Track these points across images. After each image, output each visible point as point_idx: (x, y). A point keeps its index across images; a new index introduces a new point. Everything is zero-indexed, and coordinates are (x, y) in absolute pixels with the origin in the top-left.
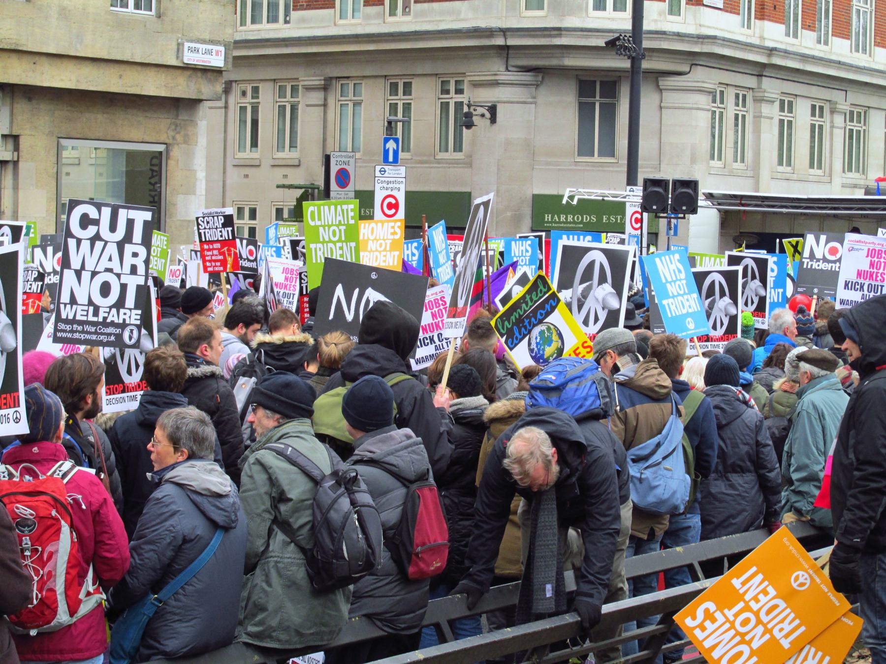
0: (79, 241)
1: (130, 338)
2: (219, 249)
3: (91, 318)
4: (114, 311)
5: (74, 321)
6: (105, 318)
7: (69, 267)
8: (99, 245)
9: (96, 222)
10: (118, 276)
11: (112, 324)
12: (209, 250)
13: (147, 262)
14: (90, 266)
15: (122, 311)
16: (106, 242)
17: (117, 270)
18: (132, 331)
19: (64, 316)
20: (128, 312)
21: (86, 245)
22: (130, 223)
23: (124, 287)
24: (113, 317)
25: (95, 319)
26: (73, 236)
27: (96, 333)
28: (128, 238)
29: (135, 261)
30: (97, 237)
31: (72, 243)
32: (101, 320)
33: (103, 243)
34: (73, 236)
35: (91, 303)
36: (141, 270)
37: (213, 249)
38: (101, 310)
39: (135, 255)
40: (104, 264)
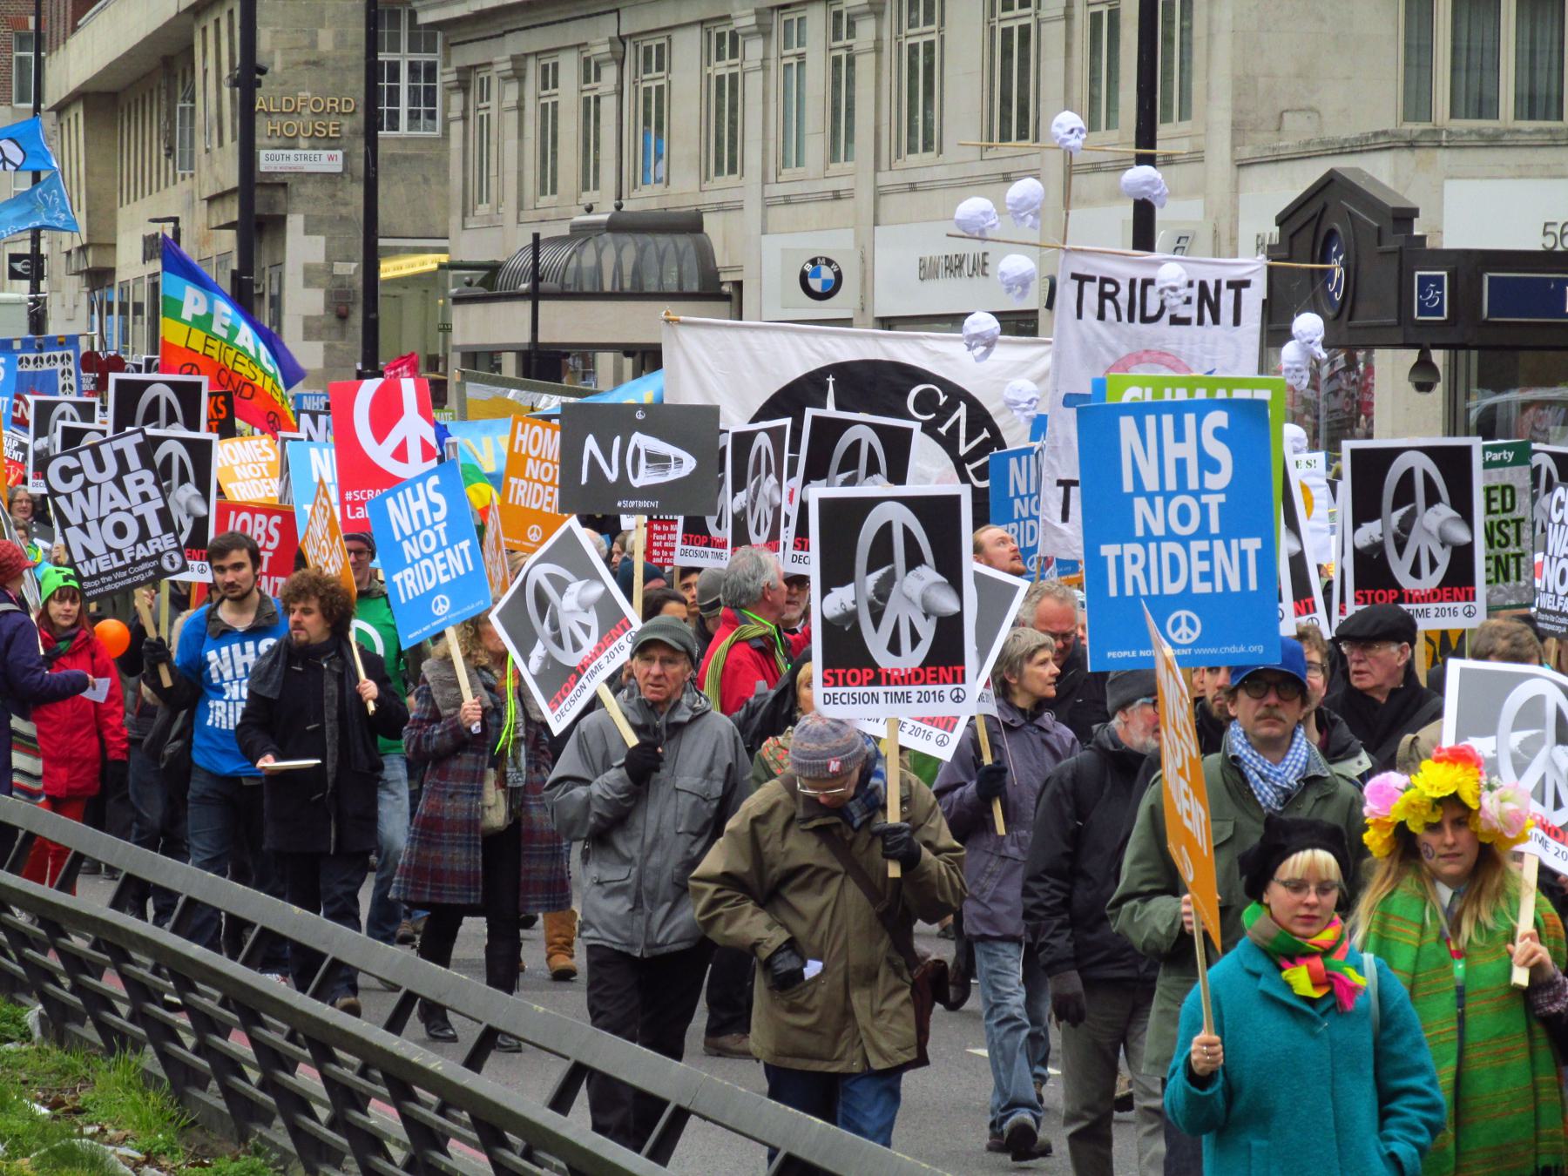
3: (117, 564)
4: (140, 546)
6: (133, 558)
11: (144, 559)
14: (92, 514)
24: (142, 552)
25: (122, 563)
26: (60, 494)
27: (129, 576)
31: (61, 501)
34: (60, 494)
35: (110, 550)
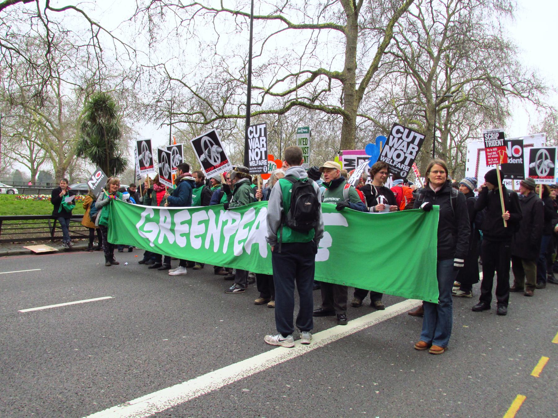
0: (394, 137)
1: (403, 175)
2: (496, 151)
3: (390, 163)
4: (399, 164)
6: (395, 165)
7: (388, 144)
8: (401, 141)
9: (402, 133)
10: (405, 153)
11: (398, 168)
12: (490, 152)
13: (417, 152)
14: (395, 146)
15: (402, 165)
16: (403, 141)
17: (405, 151)
18: (404, 173)
19: (381, 160)
20: (405, 166)
21: (396, 139)
22: (415, 138)
23: (405, 158)
24: (399, 165)
25: (392, 164)
26: (392, 135)
28: (413, 142)
29: (412, 150)
30: (401, 138)
31: (391, 137)
32: (394, 165)
33: (402, 141)
35: (392, 158)
36: (414, 154)
37: (493, 151)
38: (395, 162)
39: (413, 148)
40: (401, 147)
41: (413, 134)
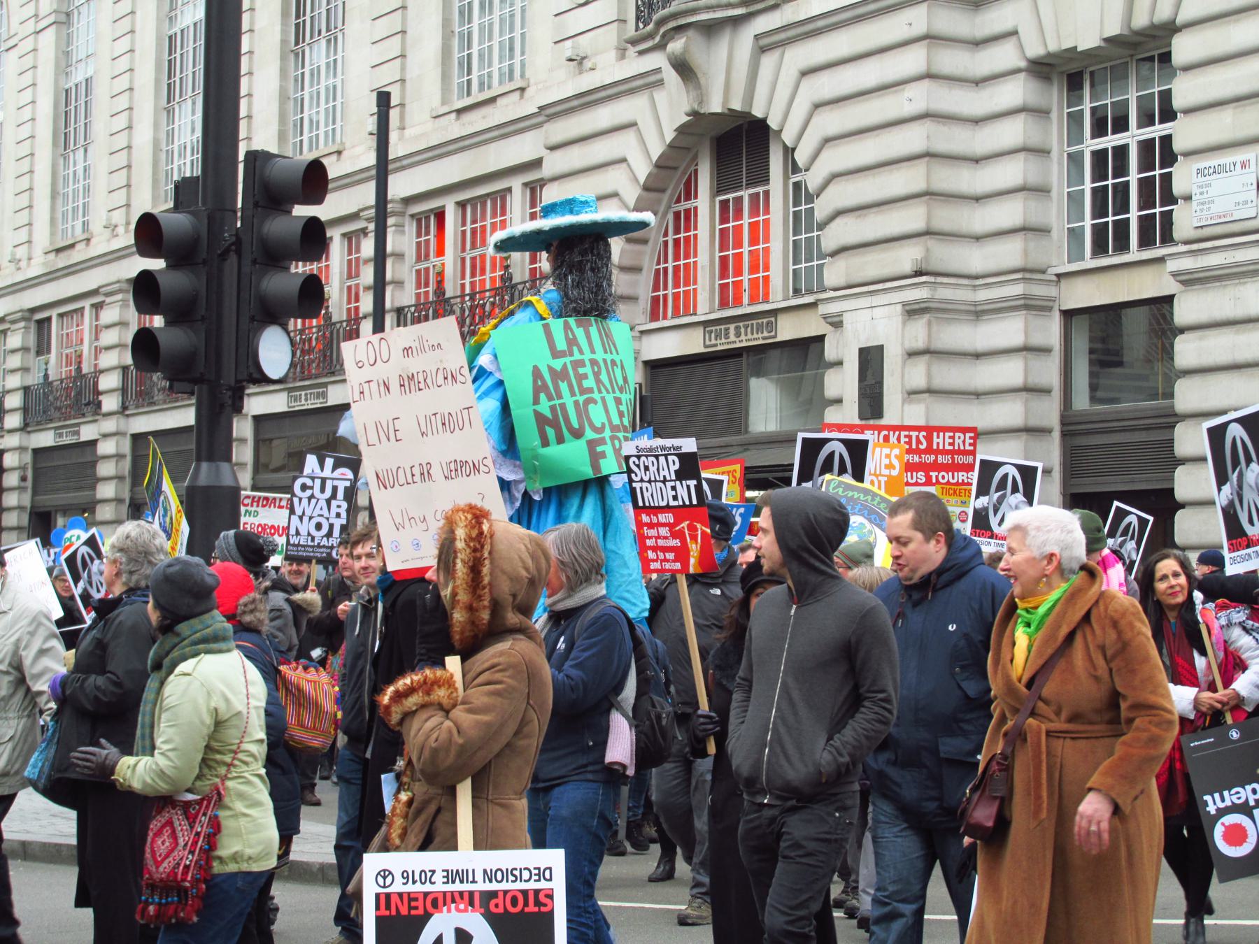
0: (300, 500)
3: (310, 543)
4: (325, 539)
5: (299, 545)
8: (313, 501)
9: (312, 488)
10: (328, 519)
14: (308, 513)
17: (326, 515)
19: (292, 542)
21: (305, 501)
22: (335, 489)
23: (331, 526)
24: (325, 542)
26: (296, 496)
28: (334, 496)
30: (312, 496)
31: (296, 500)
35: (309, 534)
37: (659, 525)
39: (339, 506)
40: (317, 511)
41: (329, 485)
